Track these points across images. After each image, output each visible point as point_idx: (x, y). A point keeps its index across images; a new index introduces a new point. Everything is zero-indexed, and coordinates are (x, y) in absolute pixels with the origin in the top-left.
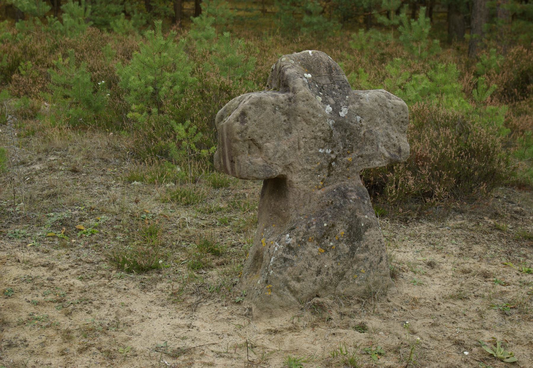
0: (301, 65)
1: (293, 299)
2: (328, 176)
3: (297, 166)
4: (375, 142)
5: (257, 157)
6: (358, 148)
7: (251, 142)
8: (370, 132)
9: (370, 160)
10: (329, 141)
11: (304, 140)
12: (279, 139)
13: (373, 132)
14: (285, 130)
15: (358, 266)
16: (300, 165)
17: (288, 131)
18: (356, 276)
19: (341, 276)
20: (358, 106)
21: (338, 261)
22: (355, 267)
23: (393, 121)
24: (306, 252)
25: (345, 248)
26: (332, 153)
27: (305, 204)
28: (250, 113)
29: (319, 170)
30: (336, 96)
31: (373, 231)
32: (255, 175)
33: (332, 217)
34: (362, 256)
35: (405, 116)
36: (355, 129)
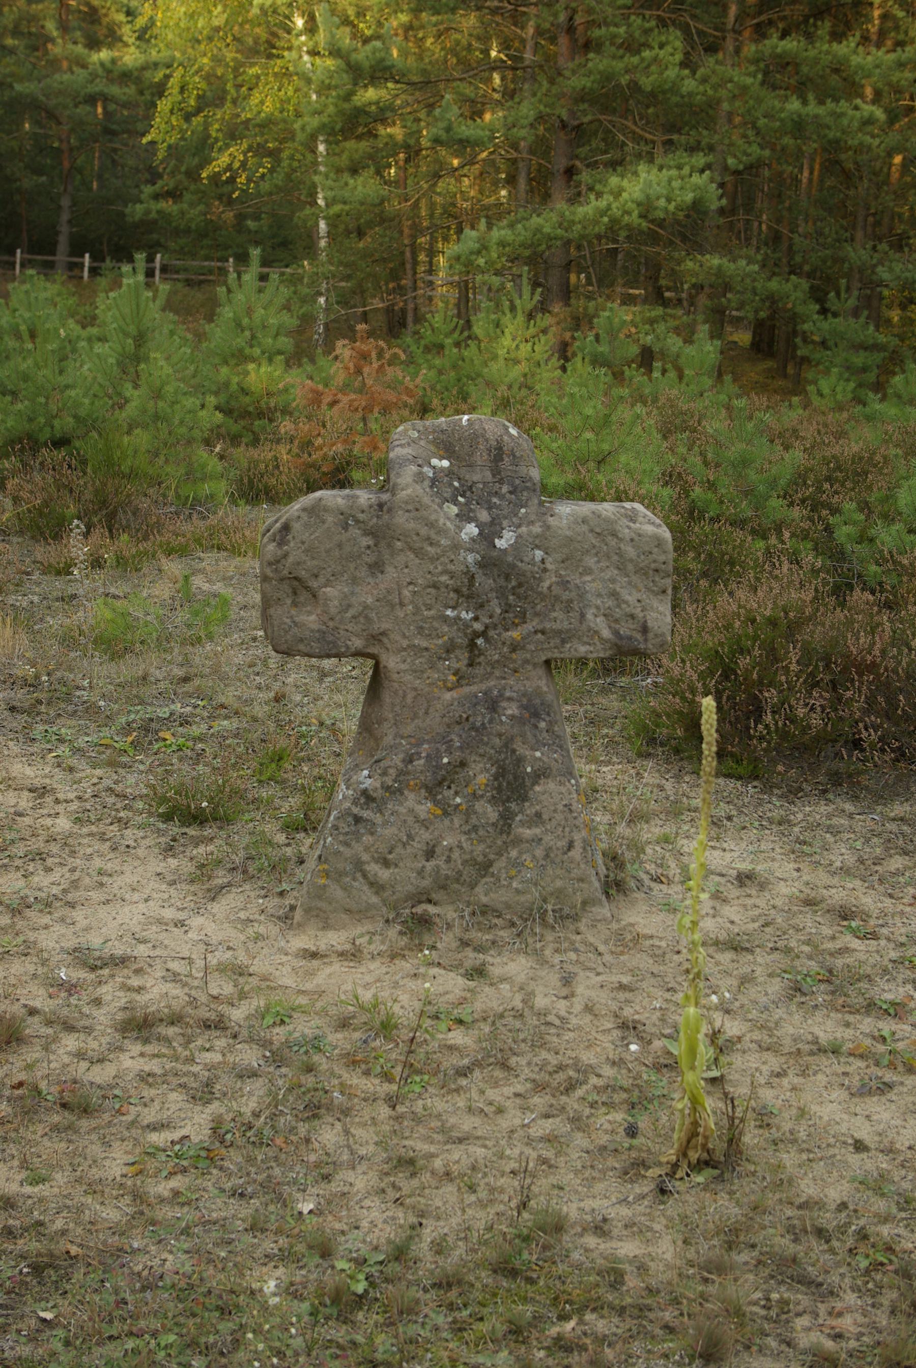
0: (434, 442)
1: (374, 899)
2: (470, 665)
3: (398, 638)
4: (575, 605)
5: (309, 613)
6: (537, 614)
7: (296, 583)
8: (564, 584)
9: (563, 642)
10: (465, 592)
11: (411, 588)
12: (354, 581)
13: (572, 586)
14: (370, 566)
15: (520, 853)
16: (404, 636)
17: (377, 567)
18: (513, 872)
19: (484, 867)
20: (539, 530)
21: (473, 835)
22: (514, 853)
23: (630, 567)
24: (402, 810)
25: (489, 812)
26: (476, 619)
27: (415, 716)
28: (296, 526)
29: (448, 651)
30: (498, 507)
31: (551, 785)
32: (301, 647)
33: (461, 748)
34: (527, 833)
35: (662, 558)
36: (529, 574)
